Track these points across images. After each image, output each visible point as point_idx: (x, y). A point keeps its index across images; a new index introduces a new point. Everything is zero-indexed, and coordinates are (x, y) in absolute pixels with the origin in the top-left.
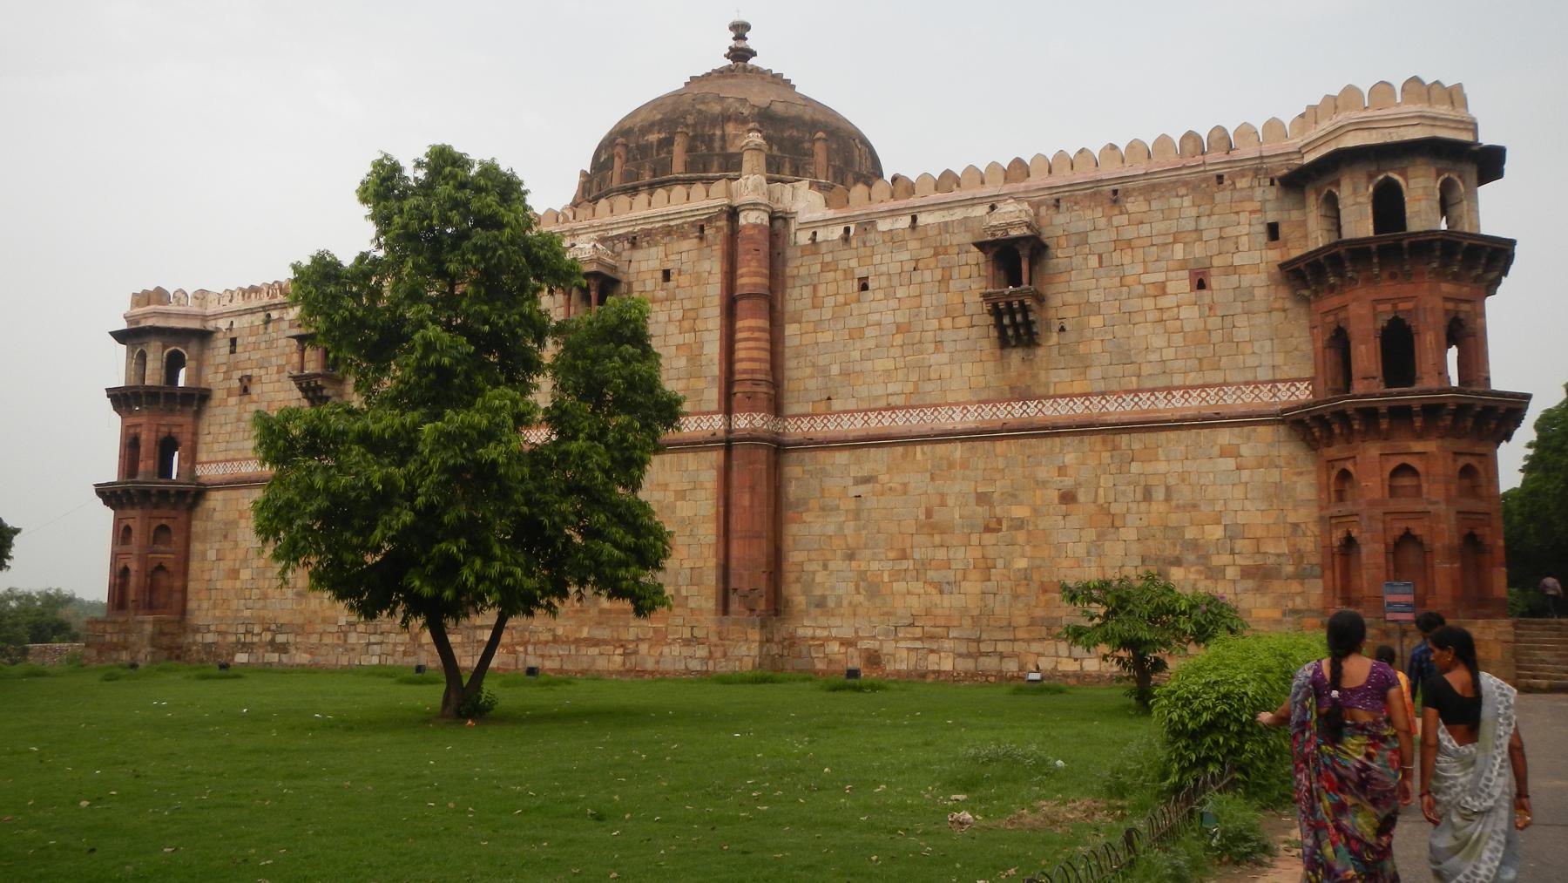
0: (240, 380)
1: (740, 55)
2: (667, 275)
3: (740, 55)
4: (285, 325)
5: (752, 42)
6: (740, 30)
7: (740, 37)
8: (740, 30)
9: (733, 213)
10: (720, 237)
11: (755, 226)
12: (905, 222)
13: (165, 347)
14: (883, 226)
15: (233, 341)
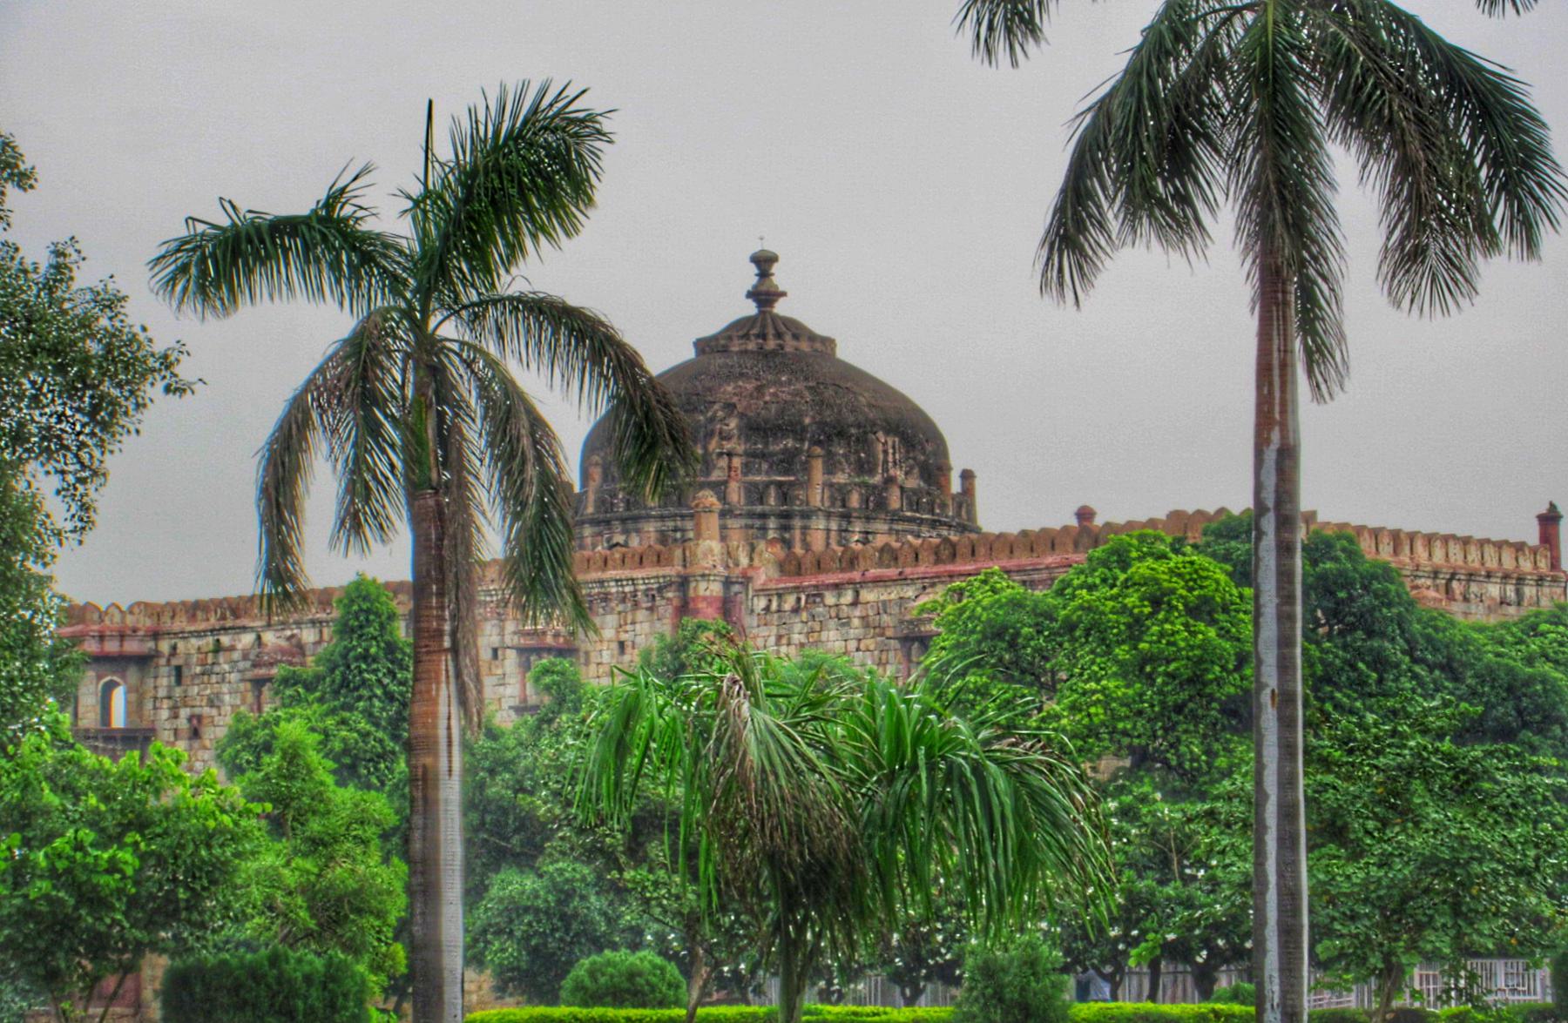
0: (190, 719)
1: (764, 296)
2: (622, 645)
3: (764, 296)
4: (236, 655)
5: (780, 276)
6: (764, 262)
7: (764, 274)
8: (764, 262)
9: (683, 583)
10: (670, 609)
11: (705, 598)
12: (848, 597)
13: (99, 678)
14: (830, 599)
15: (179, 669)
